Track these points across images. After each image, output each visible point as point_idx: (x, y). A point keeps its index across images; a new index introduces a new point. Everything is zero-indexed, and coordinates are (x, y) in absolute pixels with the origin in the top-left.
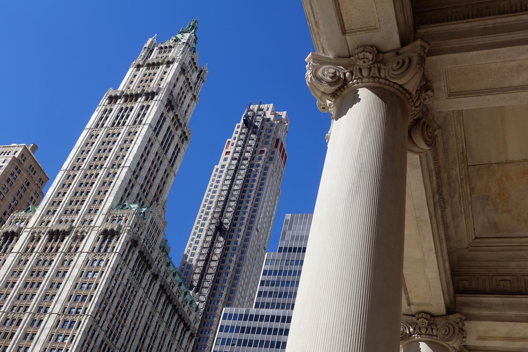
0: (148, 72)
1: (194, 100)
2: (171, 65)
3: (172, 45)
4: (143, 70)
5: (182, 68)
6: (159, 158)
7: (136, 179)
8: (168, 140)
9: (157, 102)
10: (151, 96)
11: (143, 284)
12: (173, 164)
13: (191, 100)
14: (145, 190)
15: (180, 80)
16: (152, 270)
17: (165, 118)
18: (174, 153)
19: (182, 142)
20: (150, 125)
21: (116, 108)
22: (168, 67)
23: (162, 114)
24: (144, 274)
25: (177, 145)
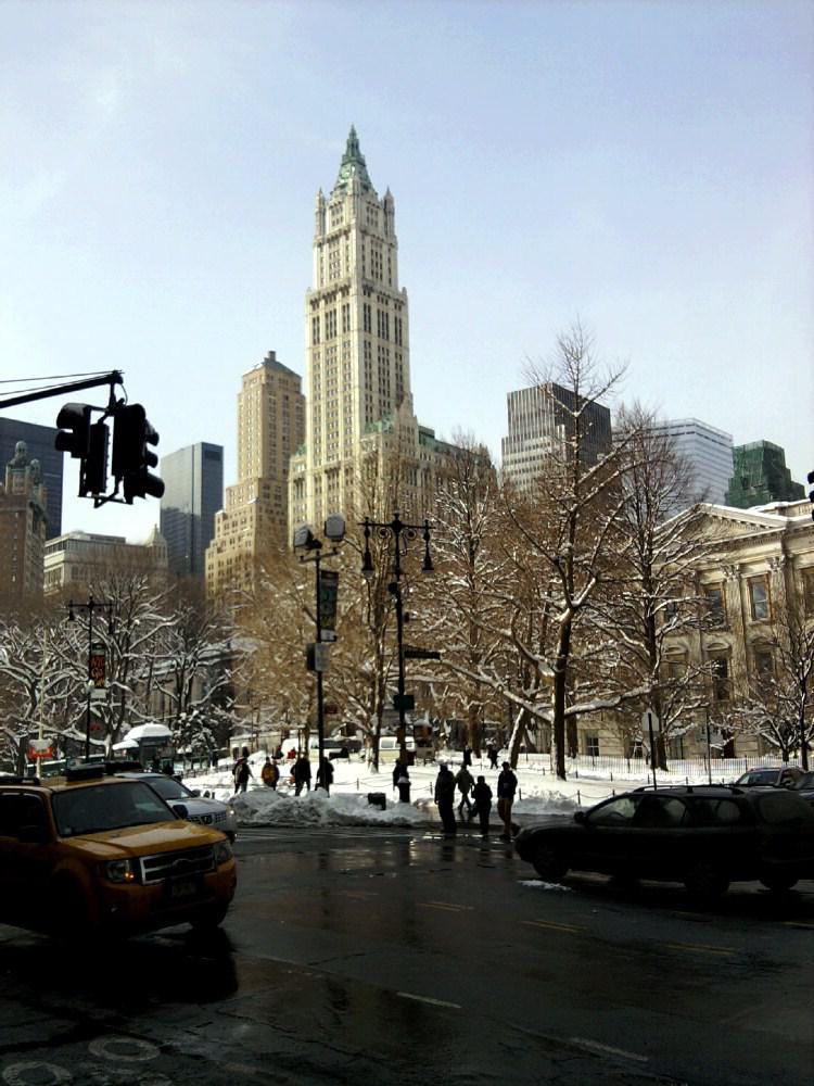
0: (333, 249)
2: (350, 234)
4: (326, 247)
11: (419, 483)
15: (366, 247)
17: (369, 308)
22: (347, 238)
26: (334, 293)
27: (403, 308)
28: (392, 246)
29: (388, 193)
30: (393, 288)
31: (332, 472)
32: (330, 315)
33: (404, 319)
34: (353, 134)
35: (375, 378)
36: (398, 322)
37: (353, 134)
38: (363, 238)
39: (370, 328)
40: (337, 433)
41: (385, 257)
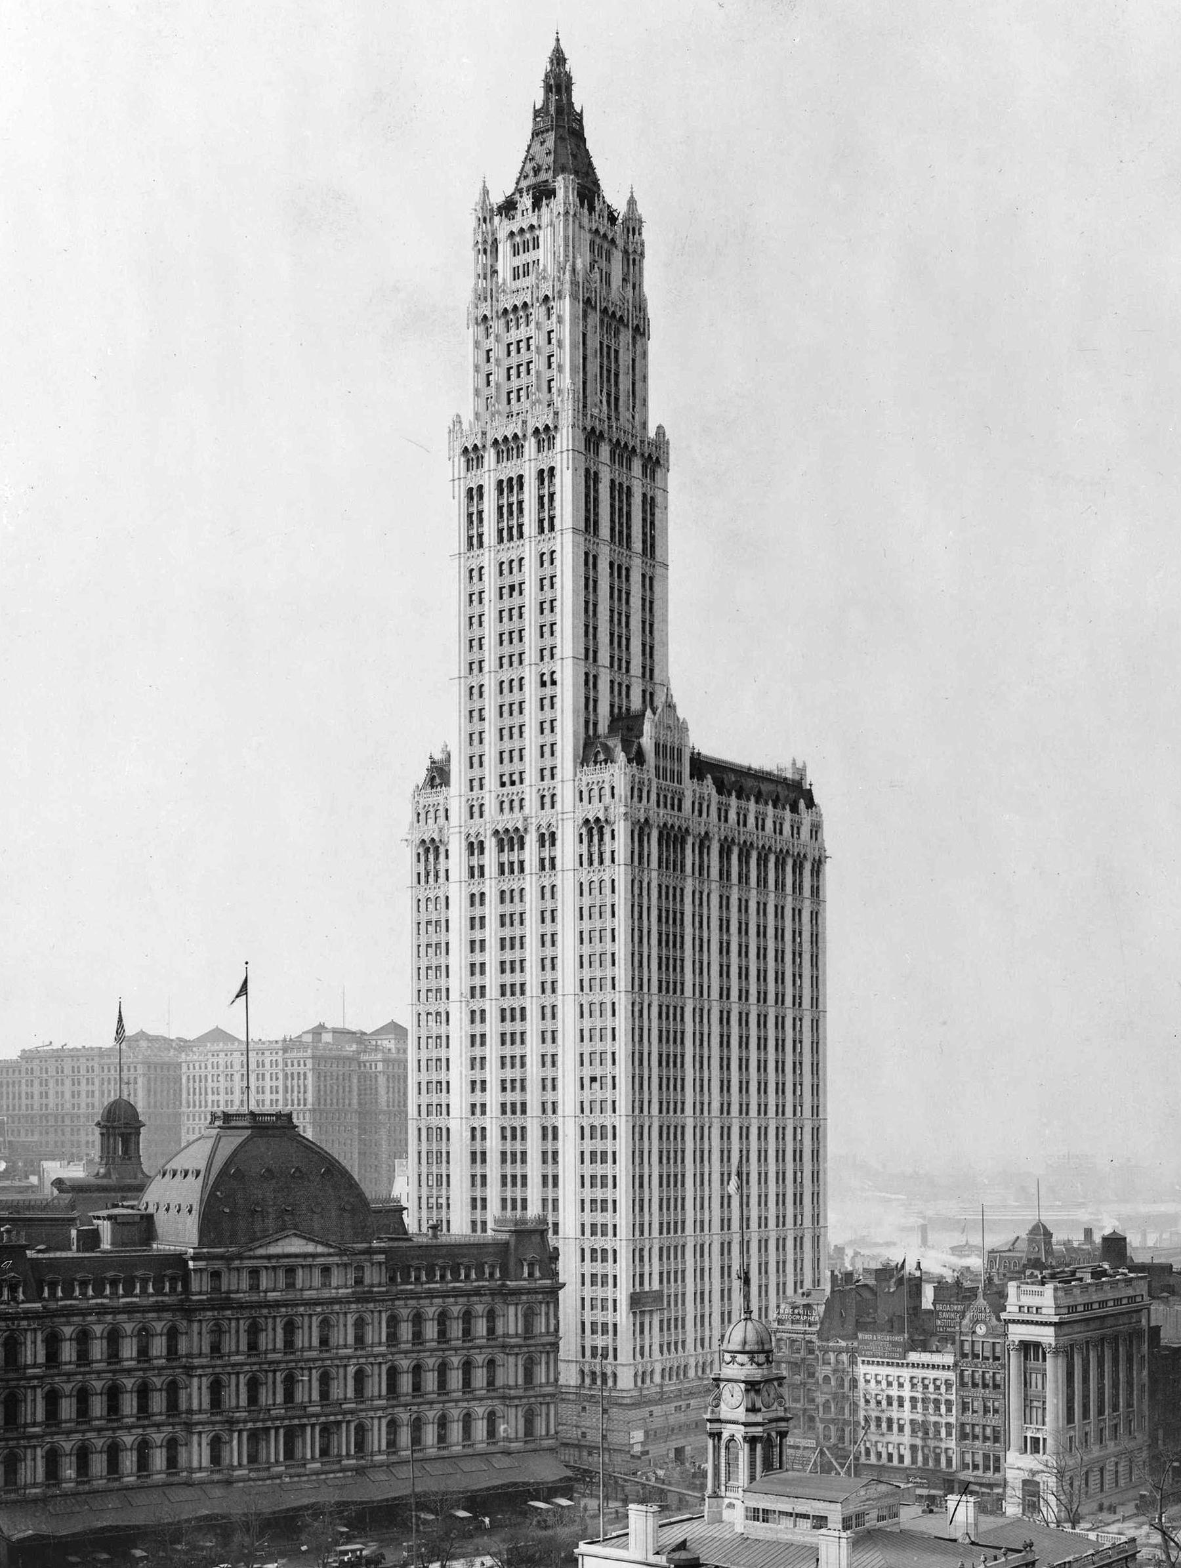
1: (638, 337)
3: (535, 223)
9: (565, 454)
10: (545, 436)
15: (589, 335)
18: (644, 520)
19: (653, 479)
20: (575, 530)
23: (587, 471)
24: (683, 850)
25: (644, 495)
28: (640, 332)
31: (510, 840)
33: (659, 500)
34: (559, 58)
36: (650, 504)
37: (559, 58)
41: (625, 358)
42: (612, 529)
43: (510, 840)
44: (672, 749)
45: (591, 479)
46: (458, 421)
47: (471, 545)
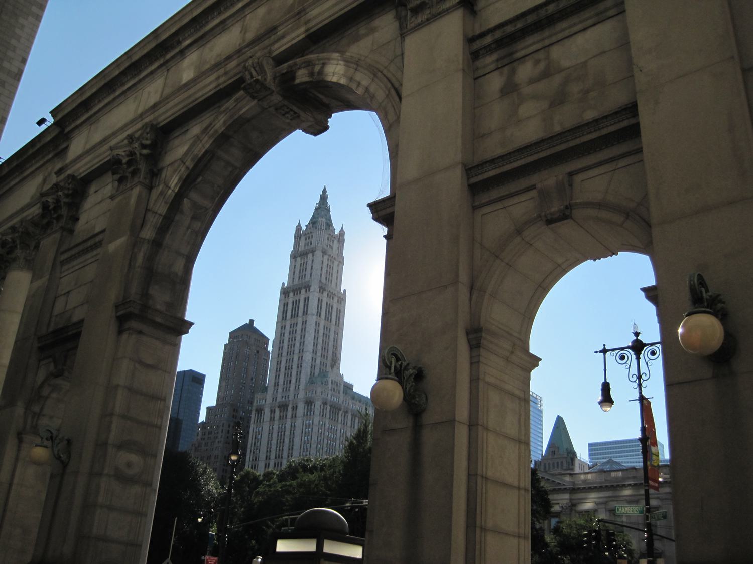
4: (299, 259)
5: (323, 252)
6: (327, 328)
7: (316, 354)
8: (329, 311)
11: (340, 421)
12: (339, 323)
13: (338, 265)
14: (324, 356)
15: (324, 261)
16: (343, 410)
19: (341, 303)
21: (290, 301)
22: (313, 255)
24: (338, 414)
26: (300, 289)
27: (342, 302)
28: (341, 262)
29: (342, 228)
30: (338, 289)
31: (283, 407)
32: (296, 303)
33: (342, 310)
34: (325, 191)
35: (320, 347)
37: (325, 191)
38: (323, 256)
39: (320, 314)
40: (290, 381)
42: (326, 316)
43: (283, 407)
44: (337, 382)
45: (320, 301)
46: (283, 284)
47: (283, 319)
